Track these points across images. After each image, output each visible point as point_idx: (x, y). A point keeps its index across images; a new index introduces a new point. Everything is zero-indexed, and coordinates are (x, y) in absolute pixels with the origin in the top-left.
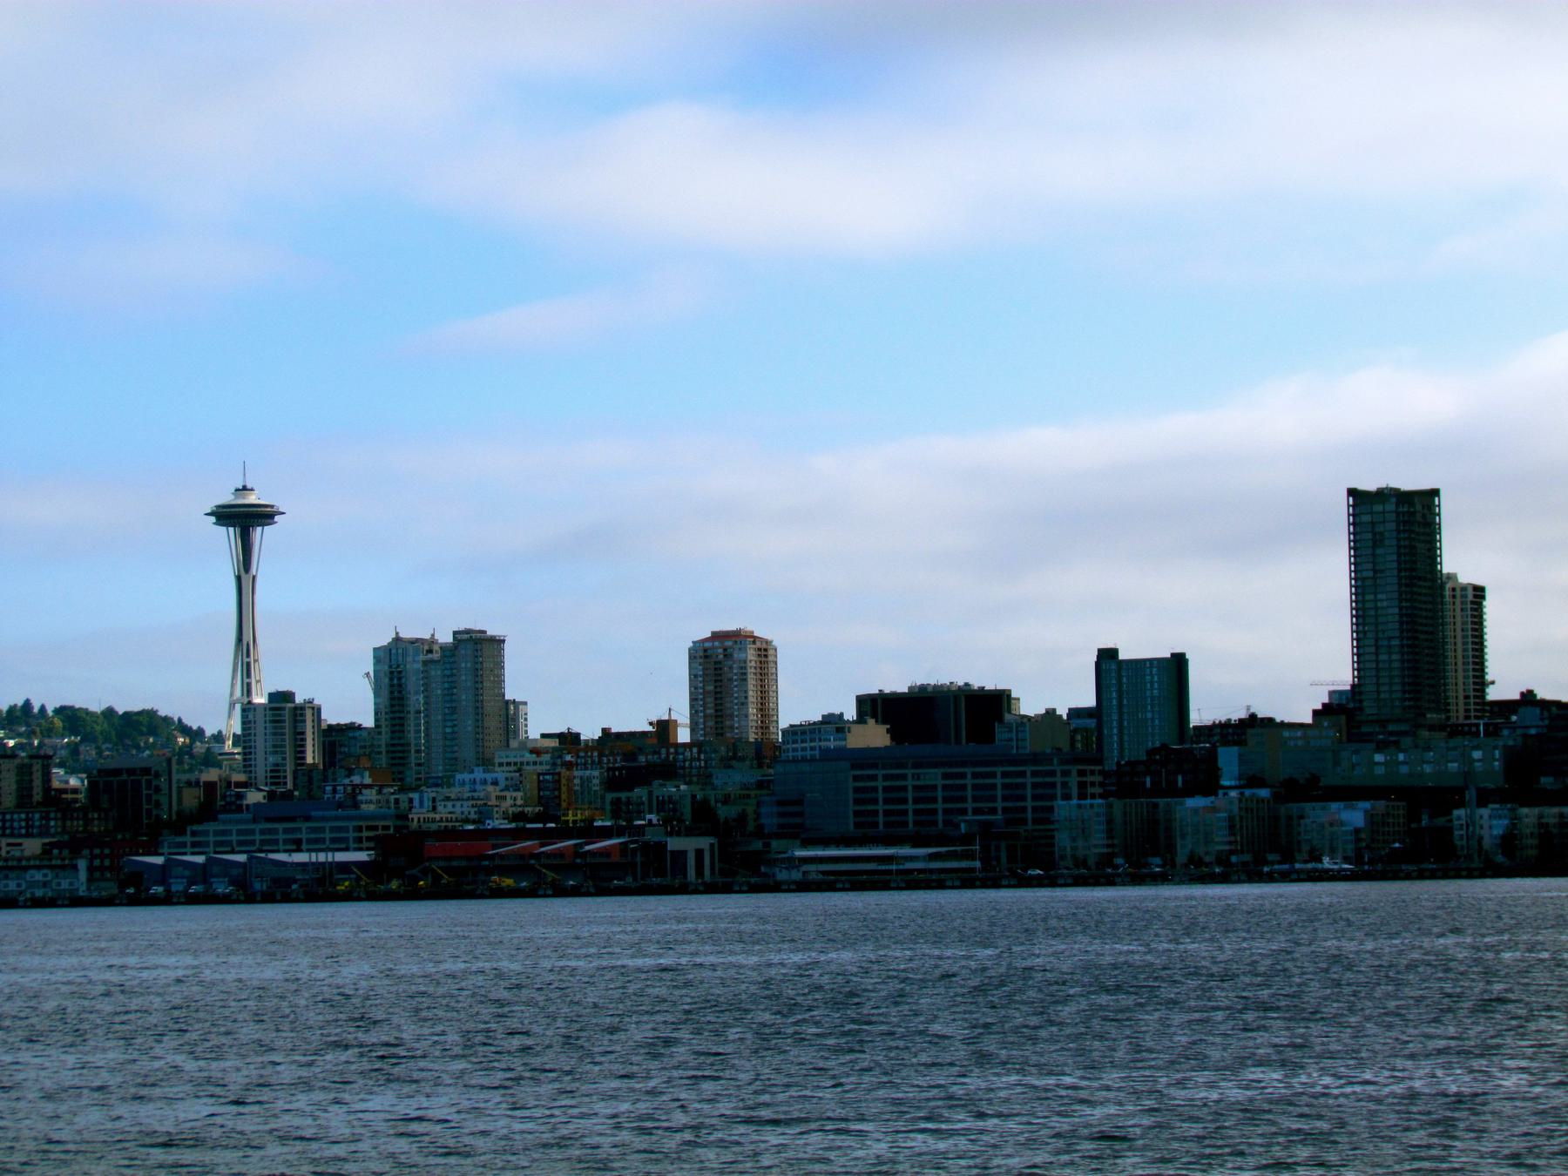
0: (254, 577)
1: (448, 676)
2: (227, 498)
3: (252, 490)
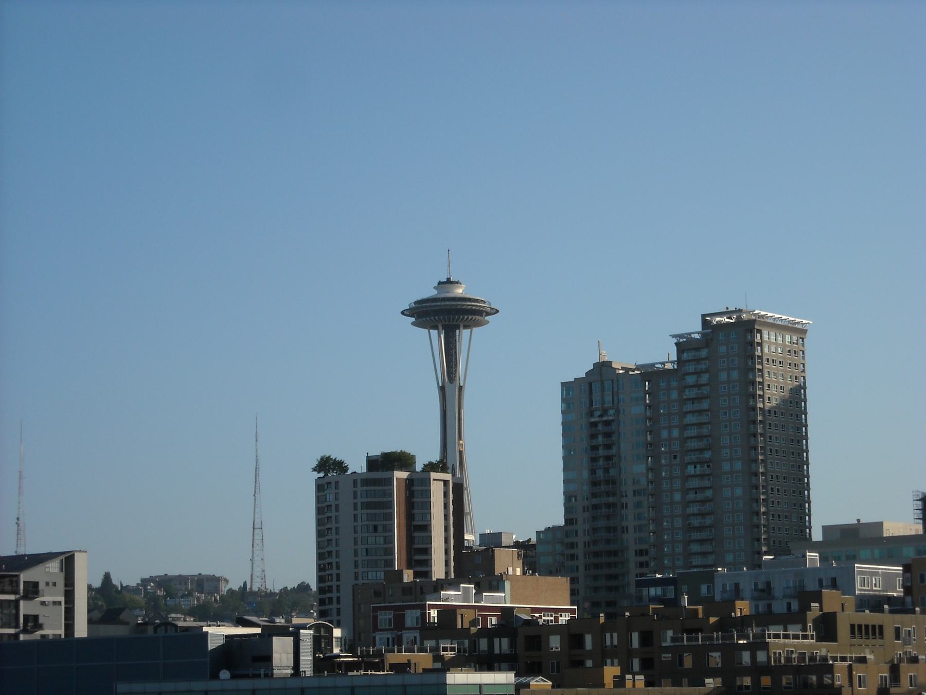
0: (461, 388)
1: (693, 400)
2: (431, 292)
3: (457, 283)
